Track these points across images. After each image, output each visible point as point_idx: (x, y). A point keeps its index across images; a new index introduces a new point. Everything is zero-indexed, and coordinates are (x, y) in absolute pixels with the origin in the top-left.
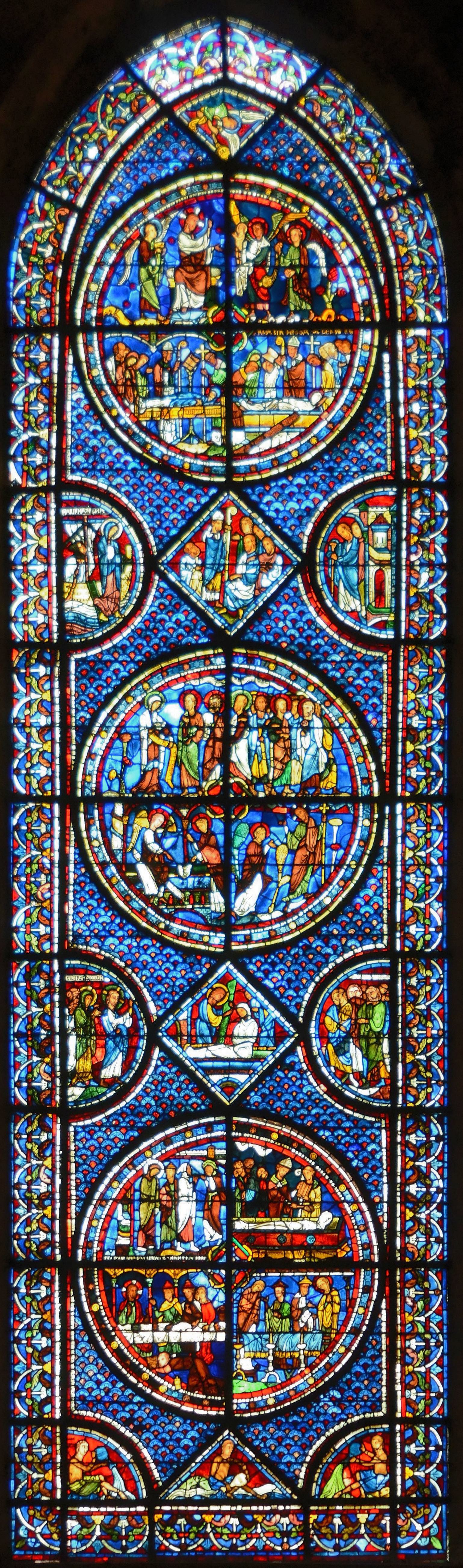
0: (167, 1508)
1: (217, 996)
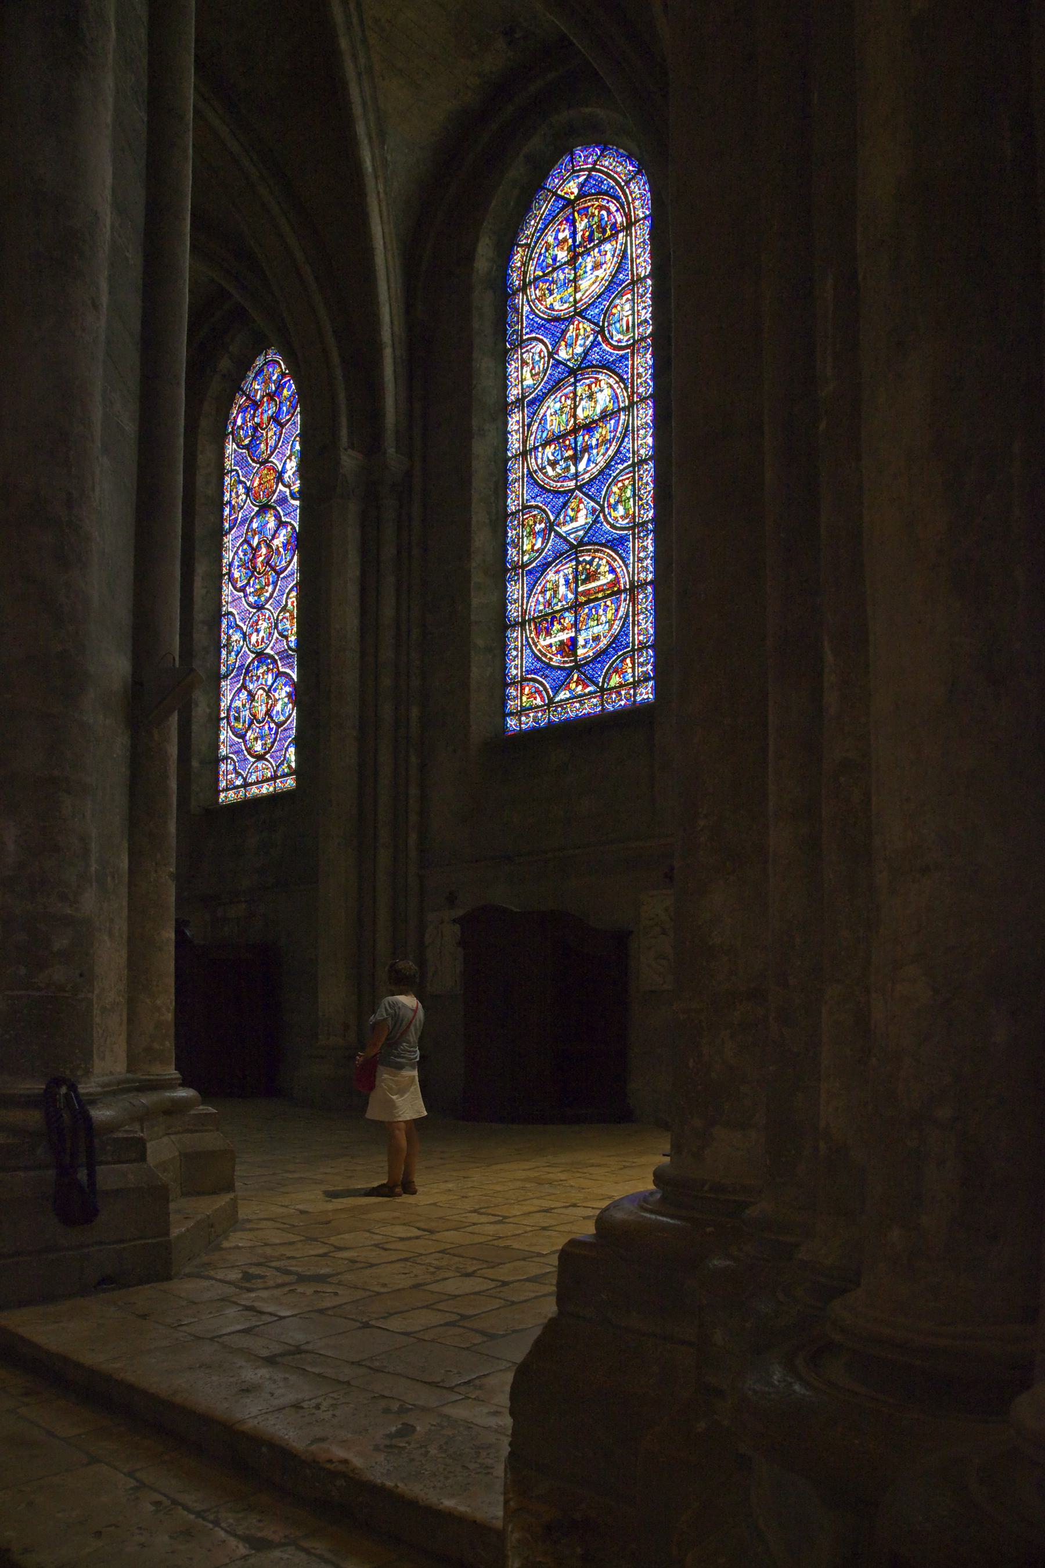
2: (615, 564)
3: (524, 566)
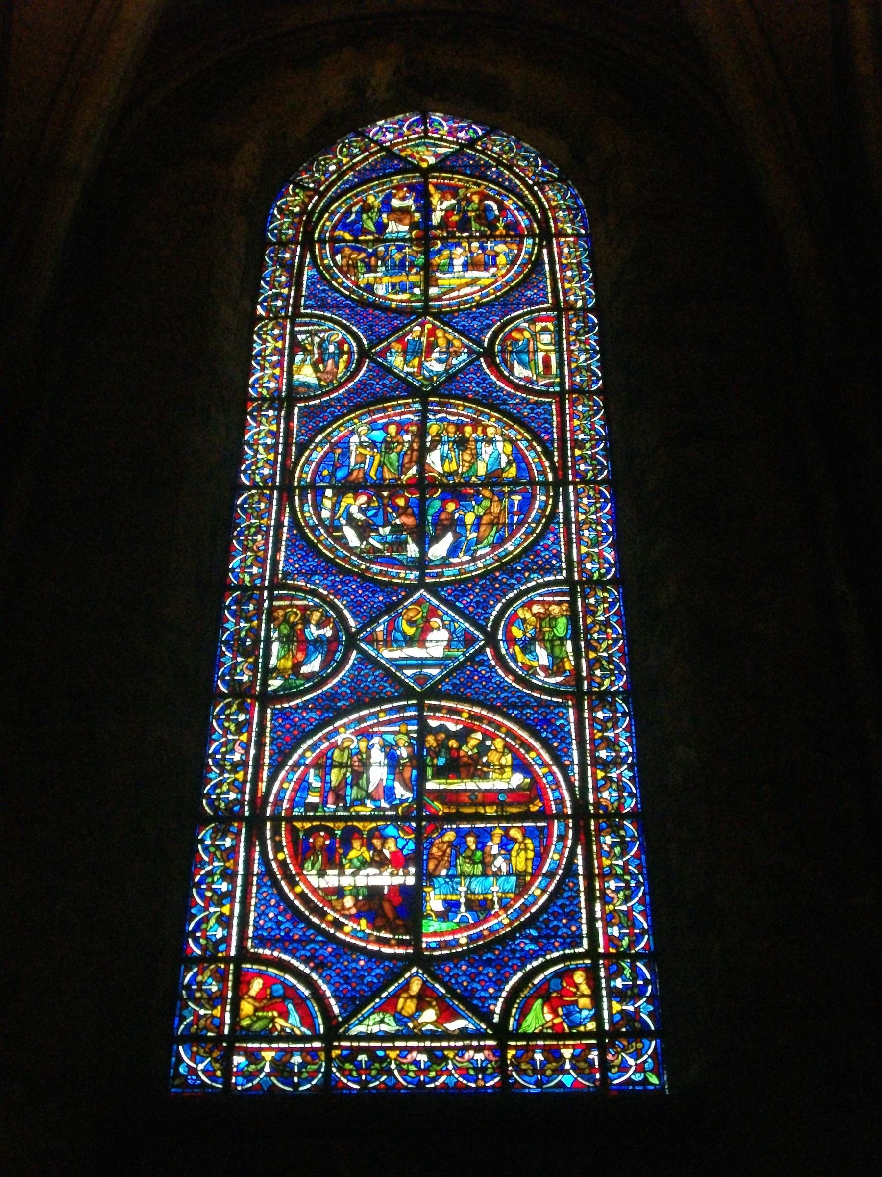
0: (348, 1044)
1: (411, 614)
2: (531, 757)
3: (267, 699)
